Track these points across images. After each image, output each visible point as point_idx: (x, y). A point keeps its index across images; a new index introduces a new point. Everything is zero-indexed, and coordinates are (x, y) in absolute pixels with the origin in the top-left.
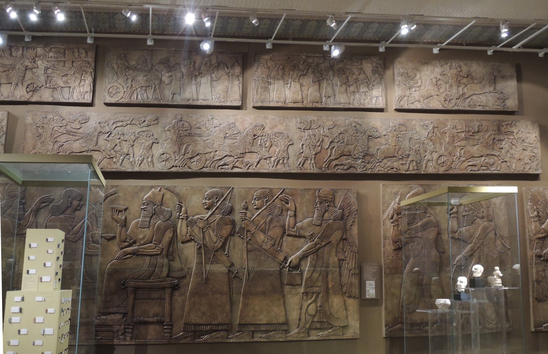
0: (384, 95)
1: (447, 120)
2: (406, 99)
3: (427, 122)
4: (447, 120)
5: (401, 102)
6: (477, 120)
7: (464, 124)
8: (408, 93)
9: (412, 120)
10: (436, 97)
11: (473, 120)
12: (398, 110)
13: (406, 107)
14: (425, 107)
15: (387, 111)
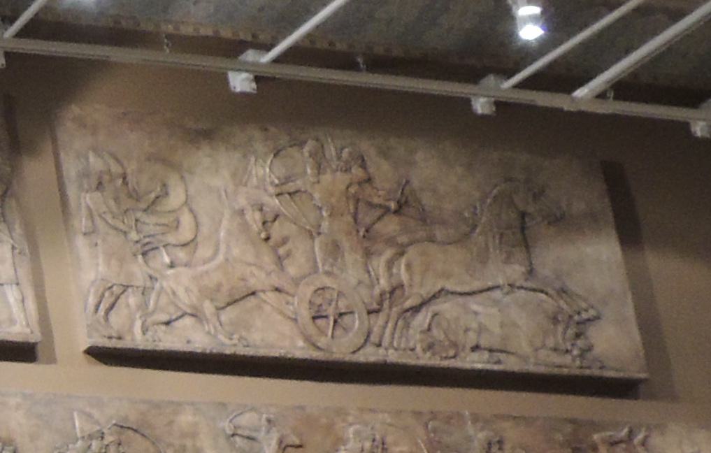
0: (24, 273)
1: (341, 412)
2: (132, 299)
3: (247, 419)
4: (341, 412)
5: (113, 314)
6: (475, 419)
7: (420, 431)
8: (138, 270)
9: (178, 406)
10: (271, 297)
11: (460, 416)
12: (104, 355)
13: (138, 340)
14: (228, 345)
15: (52, 360)
